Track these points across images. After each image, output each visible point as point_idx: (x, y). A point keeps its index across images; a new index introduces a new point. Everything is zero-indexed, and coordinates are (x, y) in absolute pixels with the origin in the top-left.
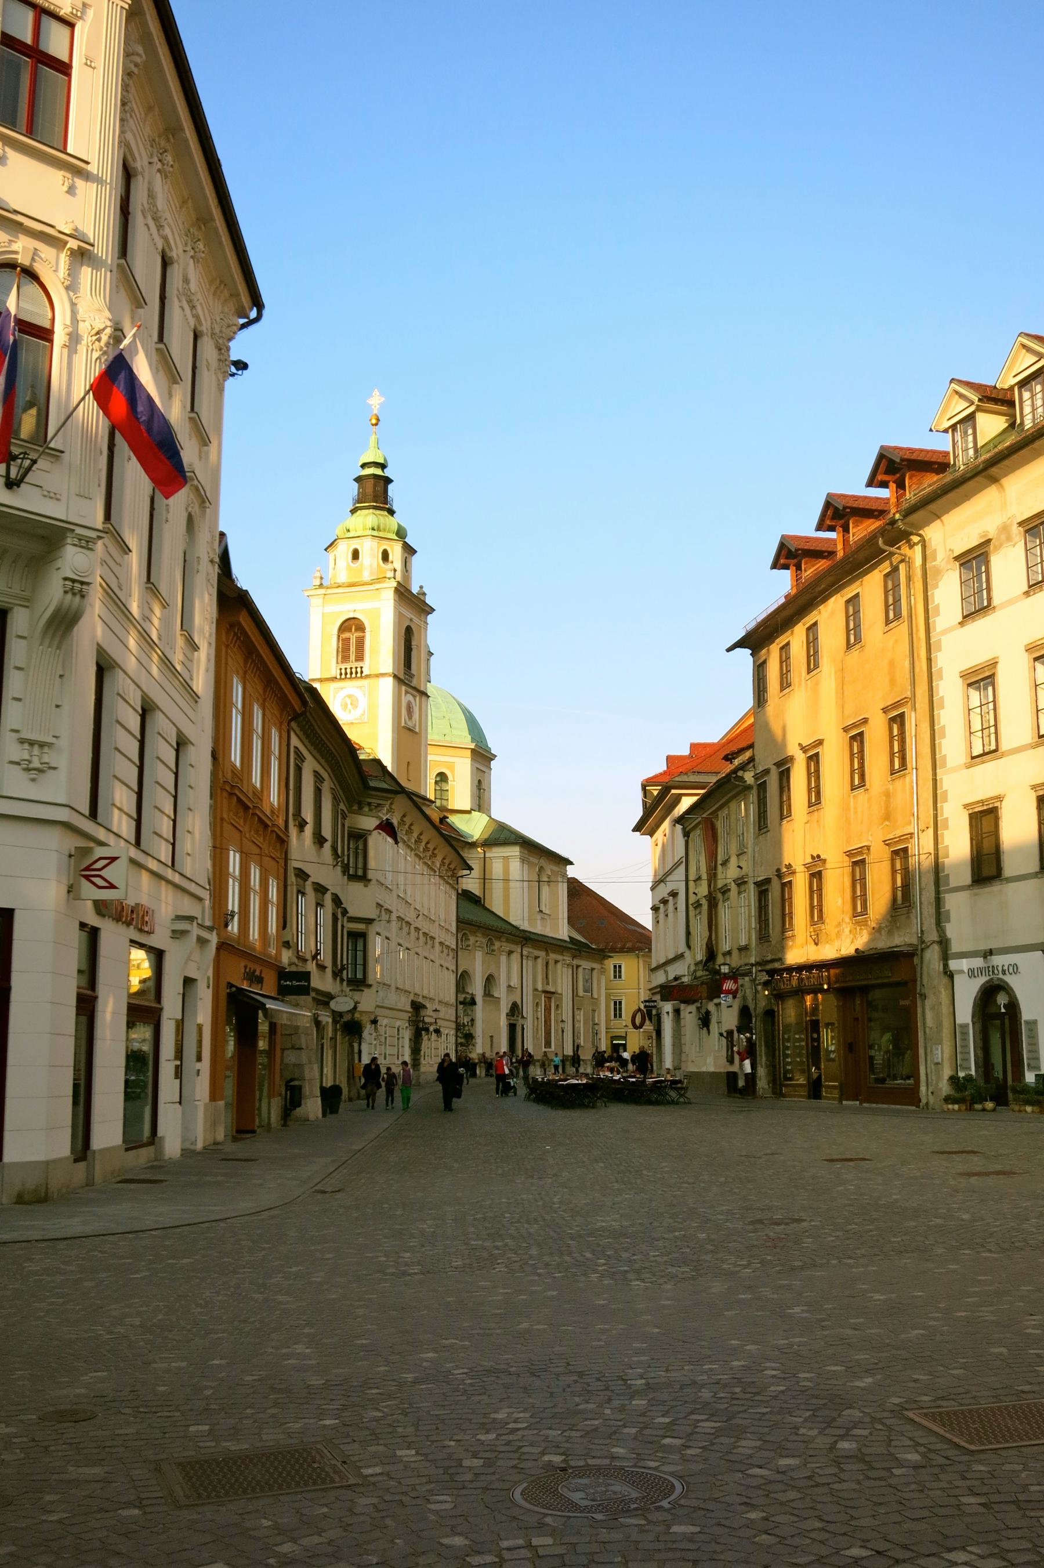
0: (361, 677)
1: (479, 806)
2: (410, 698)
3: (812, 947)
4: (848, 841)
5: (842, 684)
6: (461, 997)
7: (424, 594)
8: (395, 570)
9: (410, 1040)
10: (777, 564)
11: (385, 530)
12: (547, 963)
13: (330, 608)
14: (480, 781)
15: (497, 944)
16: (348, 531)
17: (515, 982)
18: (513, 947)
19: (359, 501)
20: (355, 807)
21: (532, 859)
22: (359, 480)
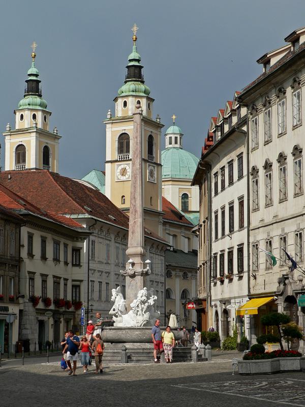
0: (128, 160)
2: (151, 168)
8: (142, 111)
11: (138, 92)
16: (123, 92)
19: (128, 78)
20: (75, 239)
22: (128, 67)
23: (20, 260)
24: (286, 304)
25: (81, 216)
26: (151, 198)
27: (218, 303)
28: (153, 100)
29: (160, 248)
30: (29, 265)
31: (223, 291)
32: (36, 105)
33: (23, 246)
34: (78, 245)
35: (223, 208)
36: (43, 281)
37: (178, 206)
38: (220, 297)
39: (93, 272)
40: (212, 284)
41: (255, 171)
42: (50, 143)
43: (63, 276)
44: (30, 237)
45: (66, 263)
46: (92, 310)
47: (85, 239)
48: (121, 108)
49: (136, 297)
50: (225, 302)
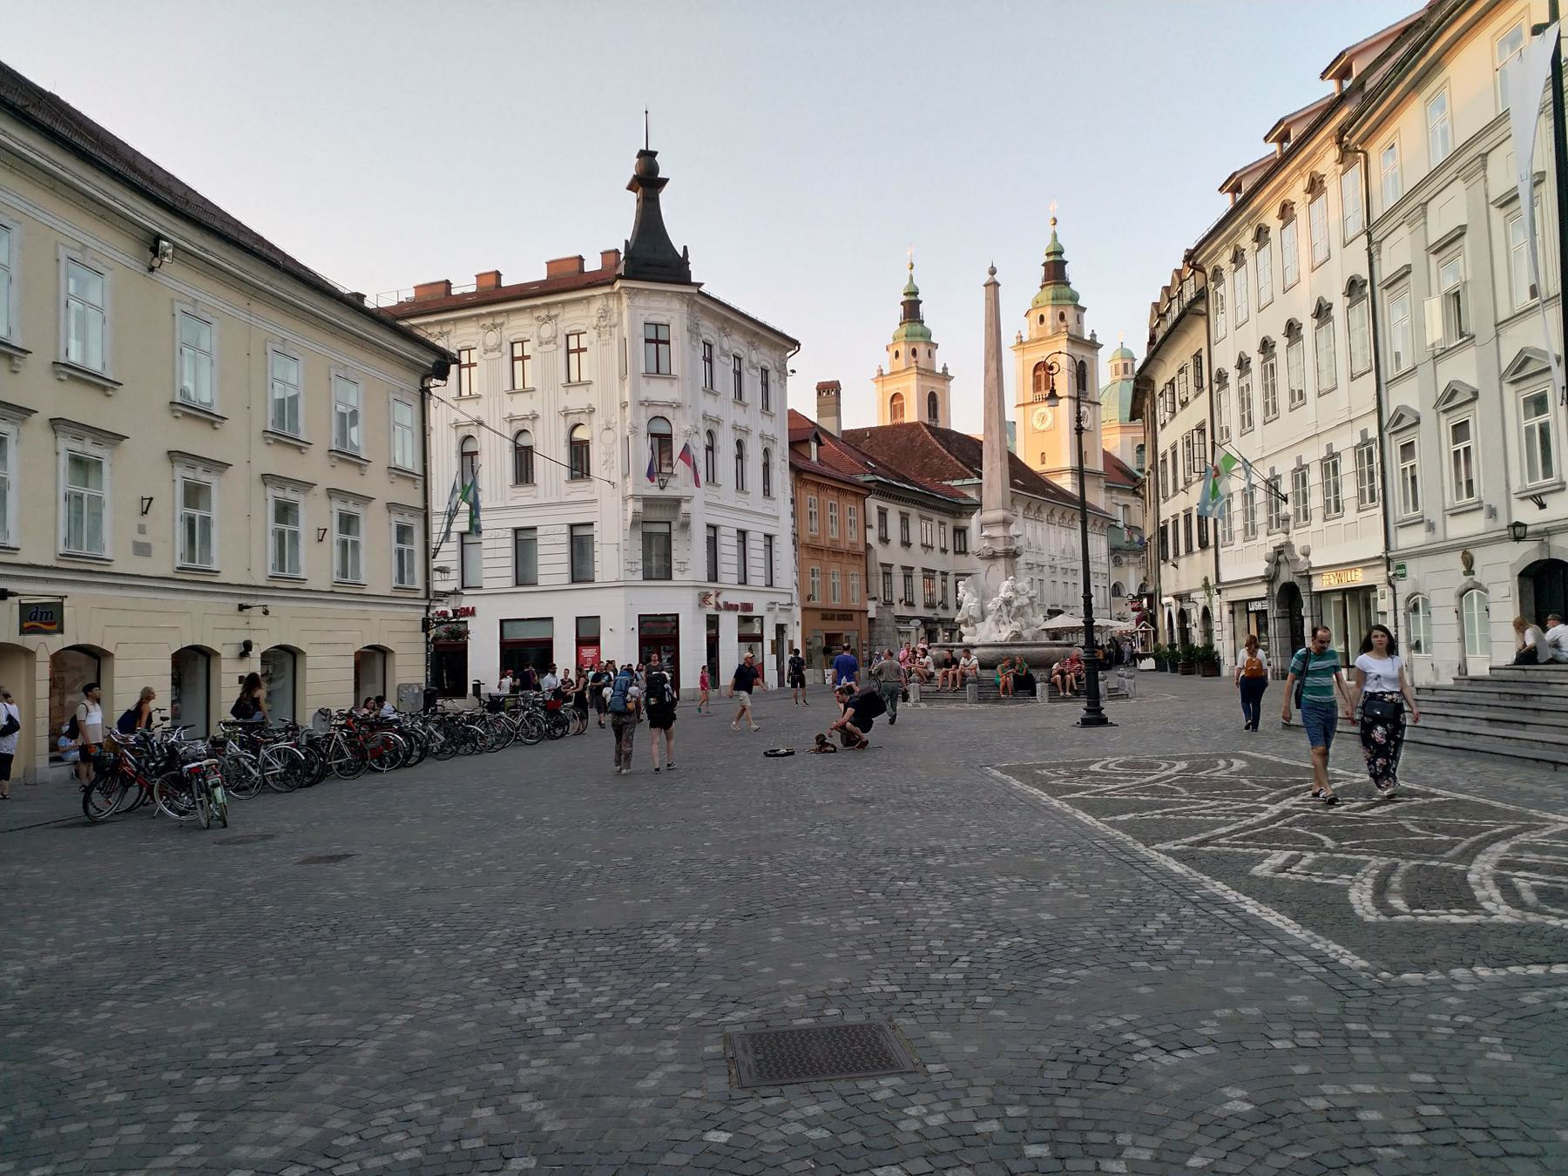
11: (1061, 299)
23: (868, 547)
24: (289, 521)
25: (967, 482)
27: (1170, 599)
28: (1084, 309)
29: (1099, 524)
30: (881, 554)
31: (1178, 581)
32: (916, 336)
33: (871, 527)
34: (963, 523)
35: (1174, 447)
36: (905, 576)
38: (1174, 591)
41: (1222, 378)
42: (936, 386)
43: (939, 567)
44: (882, 513)
45: (944, 551)
47: (972, 513)
49: (997, 593)
50: (1179, 597)
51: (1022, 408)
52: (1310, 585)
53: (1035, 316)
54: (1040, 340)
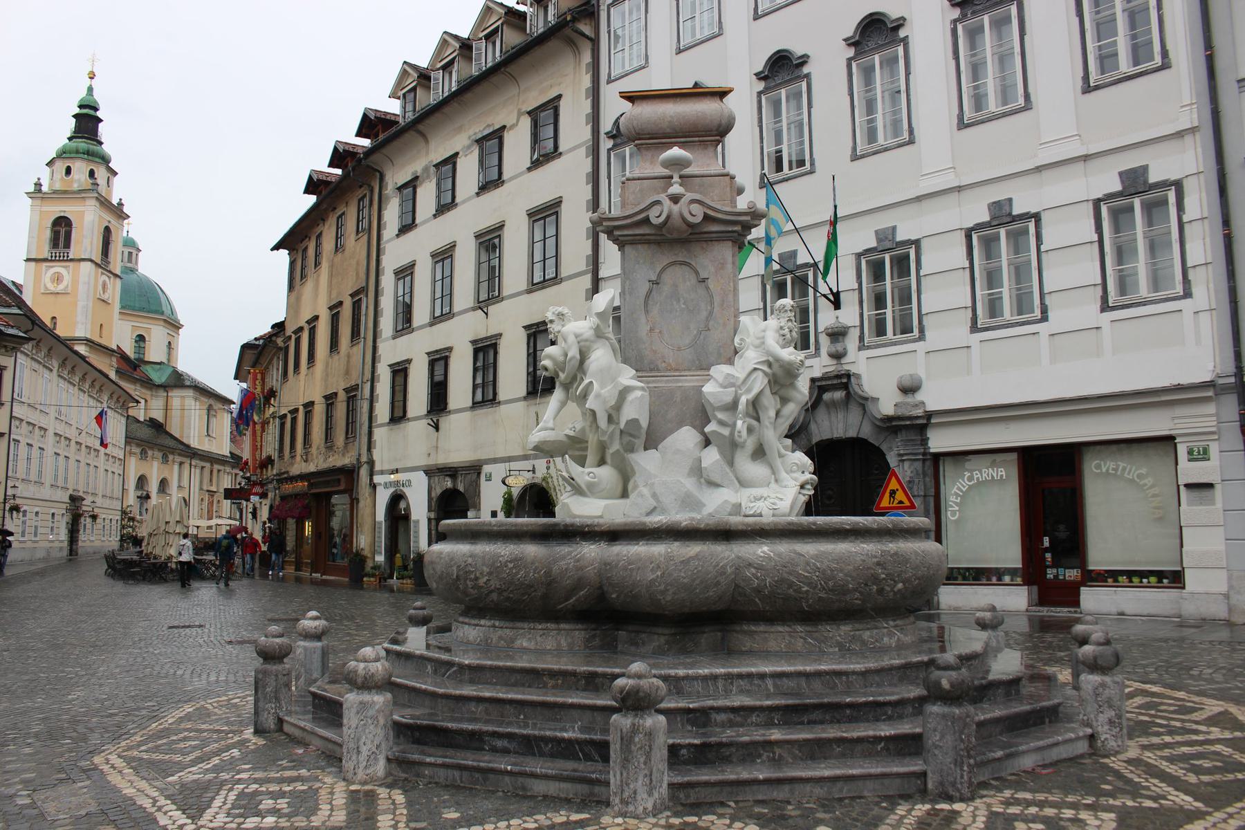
0: (67, 260)
1: (169, 360)
2: (104, 278)
3: (304, 464)
4: (326, 388)
5: (331, 276)
6: (139, 493)
7: (122, 205)
9: (68, 523)
10: (308, 191)
12: (212, 471)
13: (46, 209)
14: (169, 343)
15: (171, 457)
16: (65, 153)
17: (185, 483)
18: (184, 459)
19: (75, 132)
21: (202, 399)
26: (101, 325)
28: (115, 173)
37: (129, 350)
38: (424, 461)
39: (17, 423)
40: (379, 434)
46: (14, 496)
48: (59, 177)
51: (33, 264)
52: (924, 441)
53: (60, 166)
54: (65, 192)
